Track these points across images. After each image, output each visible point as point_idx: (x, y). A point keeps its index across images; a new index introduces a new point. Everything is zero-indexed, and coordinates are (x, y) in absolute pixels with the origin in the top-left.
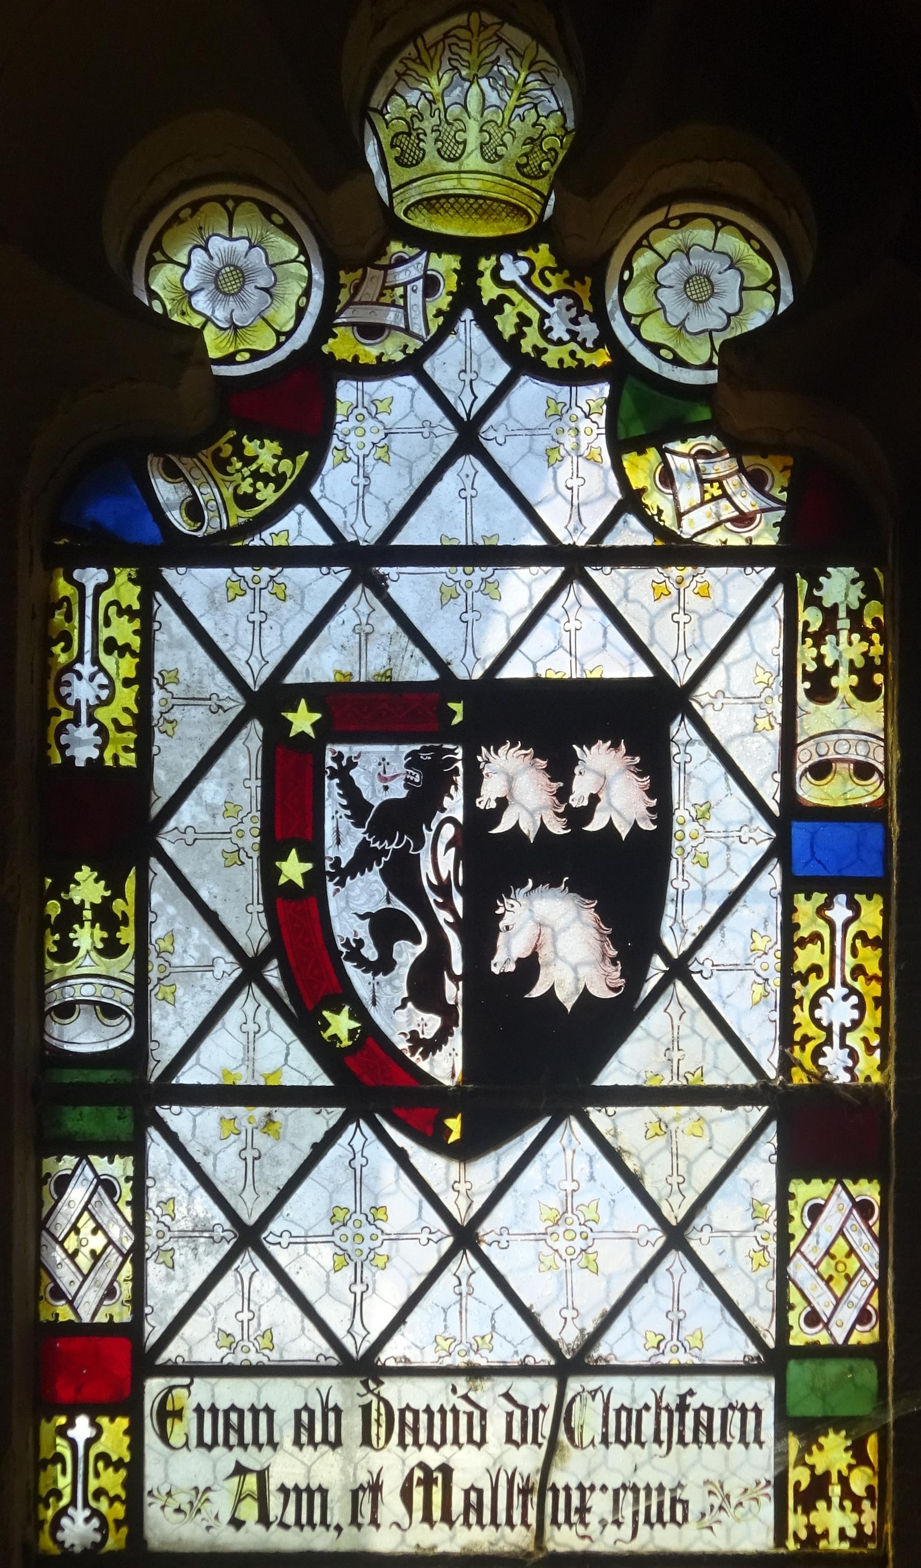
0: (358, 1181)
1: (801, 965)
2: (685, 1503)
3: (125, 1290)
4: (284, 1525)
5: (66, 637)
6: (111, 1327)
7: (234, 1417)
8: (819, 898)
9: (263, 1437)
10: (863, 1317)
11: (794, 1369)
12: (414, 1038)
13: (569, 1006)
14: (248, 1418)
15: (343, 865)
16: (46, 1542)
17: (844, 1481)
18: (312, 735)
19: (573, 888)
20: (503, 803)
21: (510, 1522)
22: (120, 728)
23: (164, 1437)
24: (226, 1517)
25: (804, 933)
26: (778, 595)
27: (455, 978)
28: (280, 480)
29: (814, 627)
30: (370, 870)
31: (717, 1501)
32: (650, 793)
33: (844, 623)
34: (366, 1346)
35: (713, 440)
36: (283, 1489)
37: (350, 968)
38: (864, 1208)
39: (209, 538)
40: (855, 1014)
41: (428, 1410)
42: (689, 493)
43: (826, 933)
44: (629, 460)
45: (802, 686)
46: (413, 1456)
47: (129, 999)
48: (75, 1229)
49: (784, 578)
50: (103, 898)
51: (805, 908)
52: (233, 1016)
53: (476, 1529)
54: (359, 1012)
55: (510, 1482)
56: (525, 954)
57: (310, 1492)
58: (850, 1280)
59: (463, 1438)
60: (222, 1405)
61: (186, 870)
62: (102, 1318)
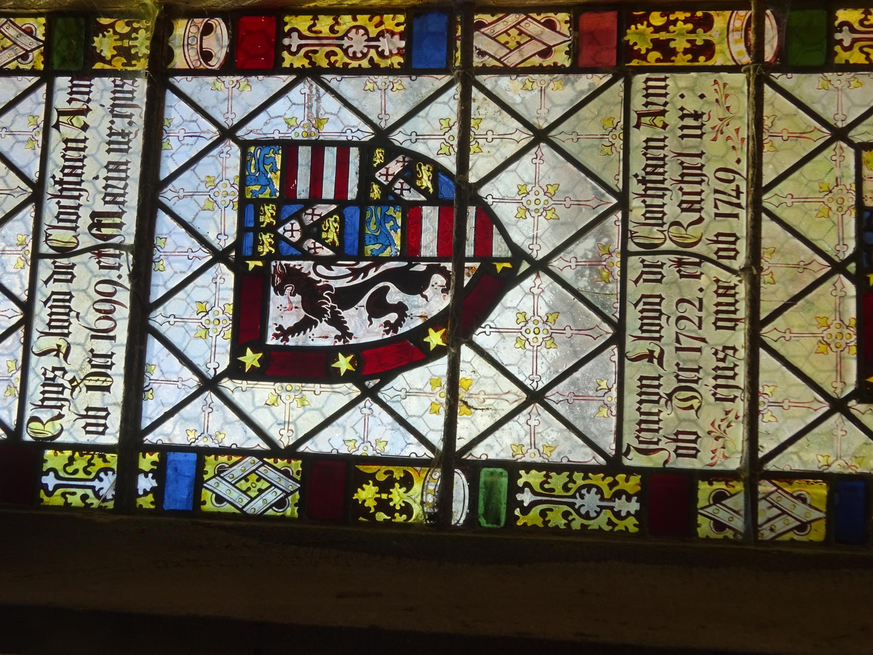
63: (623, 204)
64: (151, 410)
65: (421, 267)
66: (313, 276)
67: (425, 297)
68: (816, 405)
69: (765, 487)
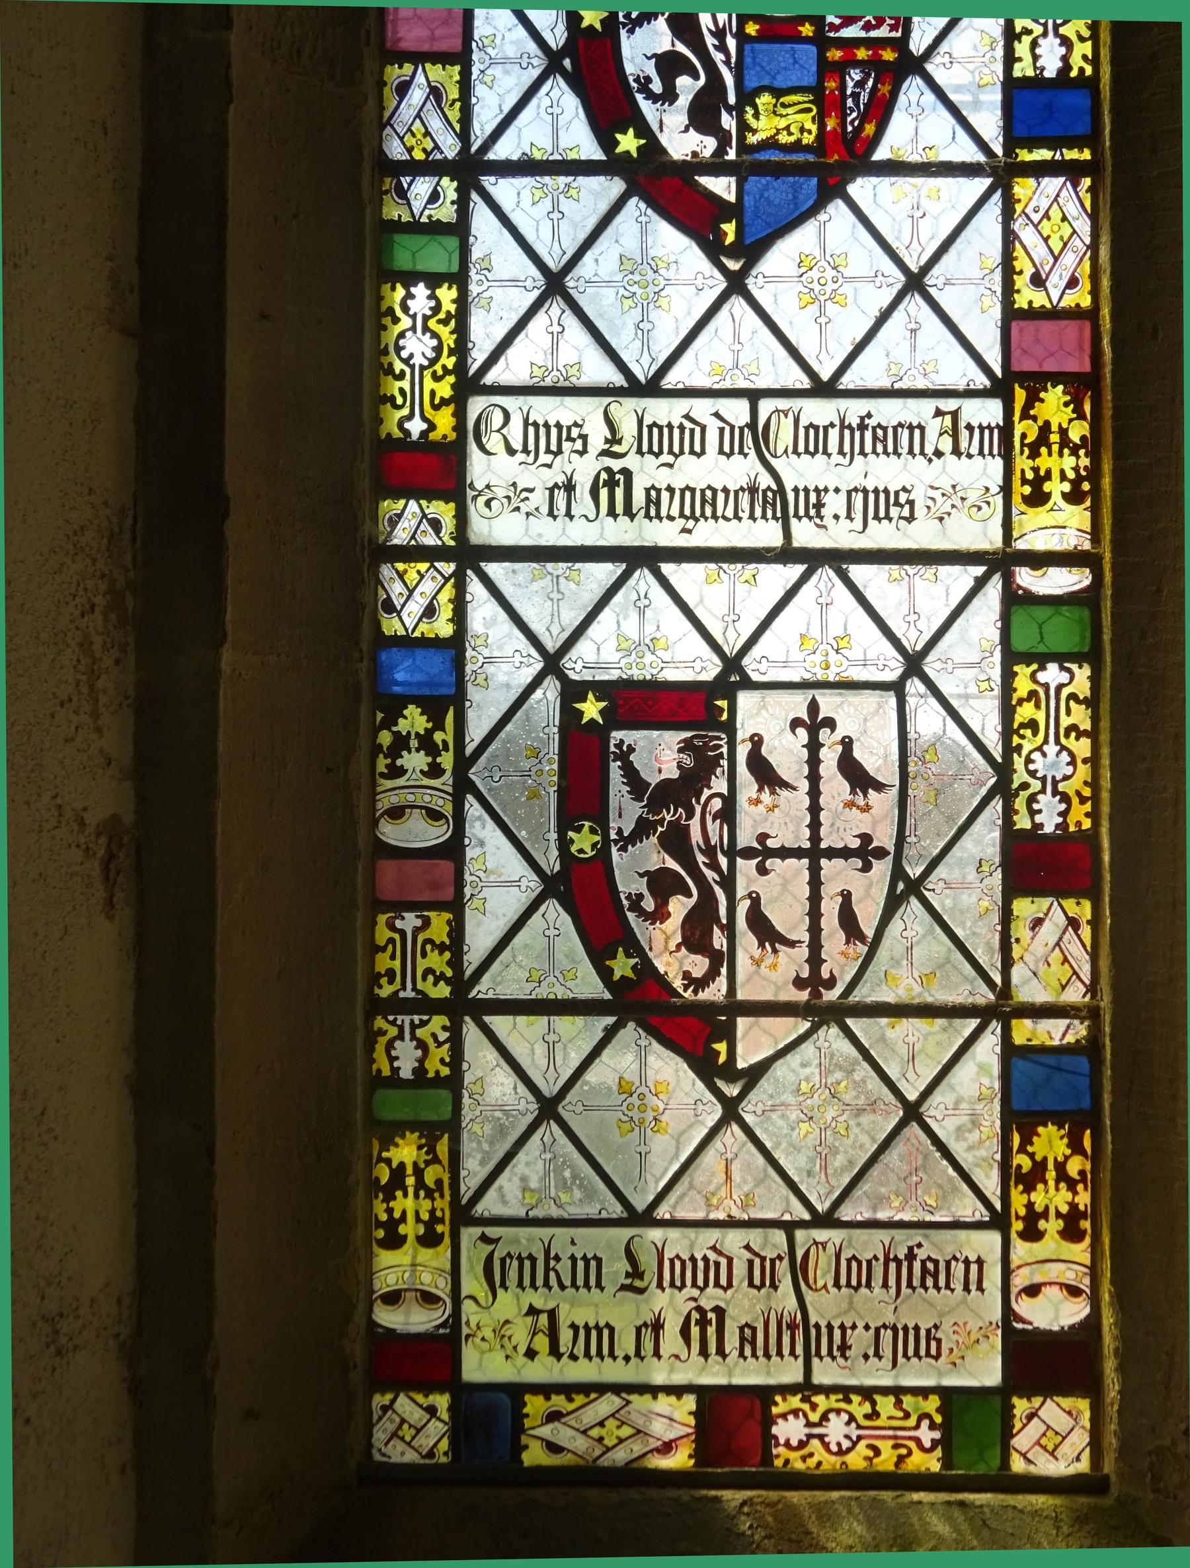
15: (626, 834)
18: (601, 721)
30: (647, 838)
50: (426, 729)
63: (824, 389)
65: (728, 122)
67: (686, 130)
68: (555, 630)
69: (448, 568)
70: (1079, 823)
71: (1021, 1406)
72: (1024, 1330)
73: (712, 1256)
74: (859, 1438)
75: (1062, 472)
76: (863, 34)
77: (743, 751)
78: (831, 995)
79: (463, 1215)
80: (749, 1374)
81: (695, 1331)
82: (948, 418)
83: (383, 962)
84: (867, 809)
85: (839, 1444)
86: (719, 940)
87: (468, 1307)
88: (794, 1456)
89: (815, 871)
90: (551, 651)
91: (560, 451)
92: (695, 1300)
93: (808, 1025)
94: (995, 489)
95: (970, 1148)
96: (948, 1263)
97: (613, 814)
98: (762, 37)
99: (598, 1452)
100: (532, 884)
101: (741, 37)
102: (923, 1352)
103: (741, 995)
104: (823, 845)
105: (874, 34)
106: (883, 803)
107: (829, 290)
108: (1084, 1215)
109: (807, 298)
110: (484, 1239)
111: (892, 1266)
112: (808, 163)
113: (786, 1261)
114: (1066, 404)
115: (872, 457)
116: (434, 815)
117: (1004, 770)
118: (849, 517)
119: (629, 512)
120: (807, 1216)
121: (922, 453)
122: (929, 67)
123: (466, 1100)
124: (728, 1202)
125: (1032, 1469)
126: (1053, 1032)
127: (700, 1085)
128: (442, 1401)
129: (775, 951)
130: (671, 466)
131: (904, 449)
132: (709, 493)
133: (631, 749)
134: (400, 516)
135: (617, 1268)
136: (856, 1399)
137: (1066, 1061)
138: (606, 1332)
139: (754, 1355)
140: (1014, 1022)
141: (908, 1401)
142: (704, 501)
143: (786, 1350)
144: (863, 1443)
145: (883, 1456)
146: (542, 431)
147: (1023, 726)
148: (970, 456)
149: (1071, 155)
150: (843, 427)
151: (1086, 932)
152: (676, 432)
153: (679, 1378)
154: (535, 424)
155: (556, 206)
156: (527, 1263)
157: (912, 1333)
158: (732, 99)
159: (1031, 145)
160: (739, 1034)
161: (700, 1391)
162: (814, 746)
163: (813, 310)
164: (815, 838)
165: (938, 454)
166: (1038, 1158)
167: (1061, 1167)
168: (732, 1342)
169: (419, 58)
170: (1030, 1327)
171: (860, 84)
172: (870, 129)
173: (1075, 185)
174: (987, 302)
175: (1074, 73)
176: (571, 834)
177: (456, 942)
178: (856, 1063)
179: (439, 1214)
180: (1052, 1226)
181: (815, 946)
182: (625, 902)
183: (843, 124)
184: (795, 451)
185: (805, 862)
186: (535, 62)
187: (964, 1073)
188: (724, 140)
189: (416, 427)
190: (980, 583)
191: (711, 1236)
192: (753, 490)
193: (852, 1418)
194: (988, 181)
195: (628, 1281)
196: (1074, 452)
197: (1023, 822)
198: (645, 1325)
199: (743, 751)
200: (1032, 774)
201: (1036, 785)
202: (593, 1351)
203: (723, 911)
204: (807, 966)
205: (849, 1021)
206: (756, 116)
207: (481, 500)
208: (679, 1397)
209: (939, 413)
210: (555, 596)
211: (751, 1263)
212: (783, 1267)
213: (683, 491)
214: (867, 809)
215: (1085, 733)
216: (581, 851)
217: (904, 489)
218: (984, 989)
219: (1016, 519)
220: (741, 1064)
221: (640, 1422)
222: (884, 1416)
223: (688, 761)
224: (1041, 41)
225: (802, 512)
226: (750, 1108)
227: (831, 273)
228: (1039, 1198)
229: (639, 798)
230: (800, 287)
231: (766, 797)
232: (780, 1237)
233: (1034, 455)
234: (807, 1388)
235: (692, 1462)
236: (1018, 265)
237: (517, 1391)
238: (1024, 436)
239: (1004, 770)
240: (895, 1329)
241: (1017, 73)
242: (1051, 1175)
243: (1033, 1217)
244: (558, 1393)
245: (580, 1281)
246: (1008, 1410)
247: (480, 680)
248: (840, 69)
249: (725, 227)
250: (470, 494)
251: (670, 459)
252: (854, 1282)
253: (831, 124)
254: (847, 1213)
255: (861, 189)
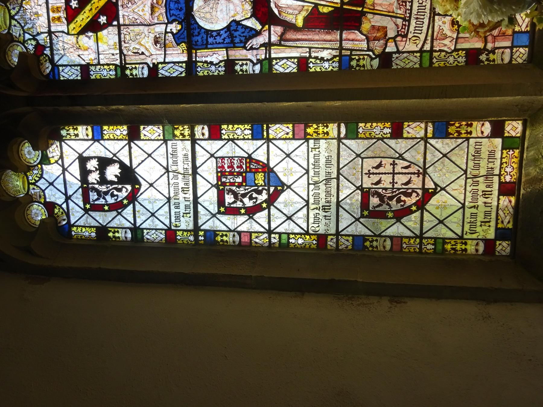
0: (145, 200)
1: (113, 138)
2: (185, 154)
3: (161, 231)
4: (190, 210)
5: (81, 237)
6: (165, 233)
7: (176, 217)
8: (104, 135)
9: (179, 213)
10: (159, 128)
11: (166, 138)
12: (126, 192)
13: (121, 171)
14: (176, 215)
16: (193, 243)
17: (181, 131)
19: (105, 170)
20: (96, 180)
21: (189, 179)
22: (91, 230)
23: (179, 227)
24: (189, 218)
25: (109, 137)
26: (66, 141)
27: (118, 186)
28: (59, 209)
29: (69, 136)
31: (185, 149)
32: (92, 159)
33: (69, 132)
34: (166, 199)
35: (48, 151)
36: (185, 211)
37: (118, 200)
38: (144, 128)
39: (67, 218)
40: (119, 130)
41: (174, 190)
42: (54, 154)
43: (108, 134)
44: (52, 162)
45: (77, 138)
46: (180, 193)
47: (124, 230)
48: (153, 238)
49: (64, 141)
51: (106, 137)
52: (125, 216)
53: (190, 184)
54: (123, 199)
55: (183, 179)
56: (114, 177)
57: (186, 207)
58: (154, 130)
59: (178, 186)
60: (175, 219)
61: (108, 222)
62: (164, 234)
63: (307, 172)
64: (200, 222)
65: (260, 188)
66: (235, 190)
70: (389, 125)
71: (506, 135)
72: (491, 134)
73: (472, 193)
74: (511, 165)
75: (322, 129)
76: (245, 165)
77: (374, 186)
78: (421, 171)
79: (461, 238)
80: (496, 186)
81: (487, 196)
82: (313, 150)
83: (412, 250)
84: (385, 164)
85: (512, 169)
86: (410, 191)
87: (479, 237)
88: (513, 178)
89: (397, 173)
90: (355, 220)
91: (319, 218)
92: (480, 196)
93: (427, 175)
94: (326, 141)
95: (453, 145)
96: (476, 149)
97: (385, 209)
98: (246, 182)
99: (510, 214)
100: (398, 224)
101: (246, 186)
102: (494, 153)
103: (421, 187)
104: (392, 172)
105: (244, 163)
106: (384, 161)
107: (289, 171)
108: (467, 123)
109: (291, 175)
110: (466, 234)
111: (476, 159)
112: (268, 175)
113: (474, 179)
114: (310, 128)
115: (320, 163)
116: (385, 241)
117: (379, 139)
118: (331, 167)
119: (330, 206)
120: (465, 175)
121: (319, 154)
122: (250, 153)
123: (439, 236)
124: (461, 190)
125: (519, 132)
126: (430, 129)
127: (438, 194)
128: (498, 243)
129: (412, 181)
130: (321, 199)
131: (318, 157)
132: (326, 192)
133: (373, 206)
134: (330, 245)
135: (474, 210)
136: (502, 166)
137: (435, 127)
138: (486, 212)
139: (492, 185)
140: (428, 137)
141: (504, 156)
142: (328, 193)
143: (491, 179)
144: (512, 165)
145: (515, 161)
146: (315, 221)
147: (370, 136)
148: (320, 146)
149: (265, 128)
150: (314, 168)
151: (410, 123)
152: (315, 198)
153: (496, 199)
154: (314, 222)
155: (276, 218)
156: (471, 226)
157: (490, 156)
158: (257, 188)
159: (263, 135)
160: (428, 187)
161: (499, 195)
162: (373, 174)
163: (293, 173)
164: (391, 173)
165: (319, 151)
166: (455, 132)
167: (457, 127)
168: (489, 189)
169: (251, 240)
170: (490, 133)
171: (253, 165)
172: (261, 164)
173: (270, 127)
174: (291, 143)
175: (250, 128)
176: (389, 217)
177: (409, 238)
178: (434, 166)
179: (461, 242)
180: (469, 129)
181: (411, 173)
182: (402, 207)
183: (260, 168)
184: (319, 177)
185: (395, 175)
186: (251, 221)
187: (437, 146)
188: (263, 189)
189: (315, 242)
190: (343, 144)
191: (468, 193)
192: (326, 184)
193: (506, 167)
194: (270, 143)
195: (476, 208)
196: (319, 127)
197: (389, 135)
198: (485, 205)
199: (374, 186)
200: (379, 134)
201: (381, 133)
202: (490, 215)
203: (404, 190)
204: (415, 175)
205: (426, 167)
206: (259, 183)
207: (328, 231)
208: (500, 199)
209: (312, 151)
210: (345, 219)
211: (473, 186)
212: (475, 180)
213: (326, 197)
214: (385, 164)
215: (372, 124)
216: (392, 215)
217: (326, 157)
218: (421, 142)
219: (331, 137)
220: (434, 187)
221: (504, 206)
222: (506, 161)
223: (376, 196)
224: (245, 134)
225: (330, 176)
226: (442, 185)
227: (287, 171)
228: (463, 132)
229: (382, 205)
230: (289, 176)
231: (383, 182)
232: (468, 180)
233: (319, 134)
234: (500, 175)
235: (513, 197)
236: (285, 137)
237: (497, 229)
238: (316, 136)
239: (379, 139)
240: (488, 159)
241: (250, 138)
242: (458, 129)
243: (467, 133)
244: (498, 221)
245: (475, 217)
246: (507, 137)
247: (360, 232)
248: (251, 169)
249: (279, 189)
250: (326, 233)
251: (320, 199)
252: (478, 166)
253: (260, 170)
254: (464, 168)
255: (272, 165)
